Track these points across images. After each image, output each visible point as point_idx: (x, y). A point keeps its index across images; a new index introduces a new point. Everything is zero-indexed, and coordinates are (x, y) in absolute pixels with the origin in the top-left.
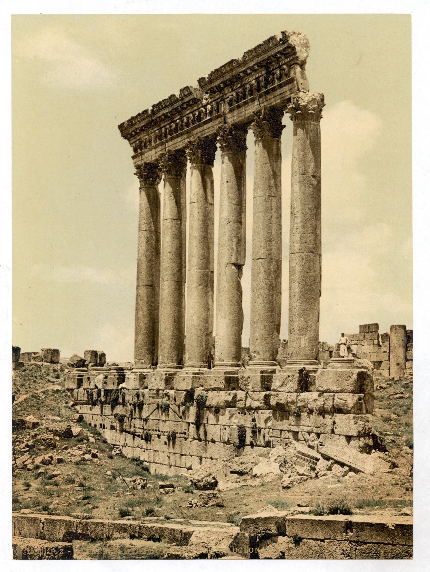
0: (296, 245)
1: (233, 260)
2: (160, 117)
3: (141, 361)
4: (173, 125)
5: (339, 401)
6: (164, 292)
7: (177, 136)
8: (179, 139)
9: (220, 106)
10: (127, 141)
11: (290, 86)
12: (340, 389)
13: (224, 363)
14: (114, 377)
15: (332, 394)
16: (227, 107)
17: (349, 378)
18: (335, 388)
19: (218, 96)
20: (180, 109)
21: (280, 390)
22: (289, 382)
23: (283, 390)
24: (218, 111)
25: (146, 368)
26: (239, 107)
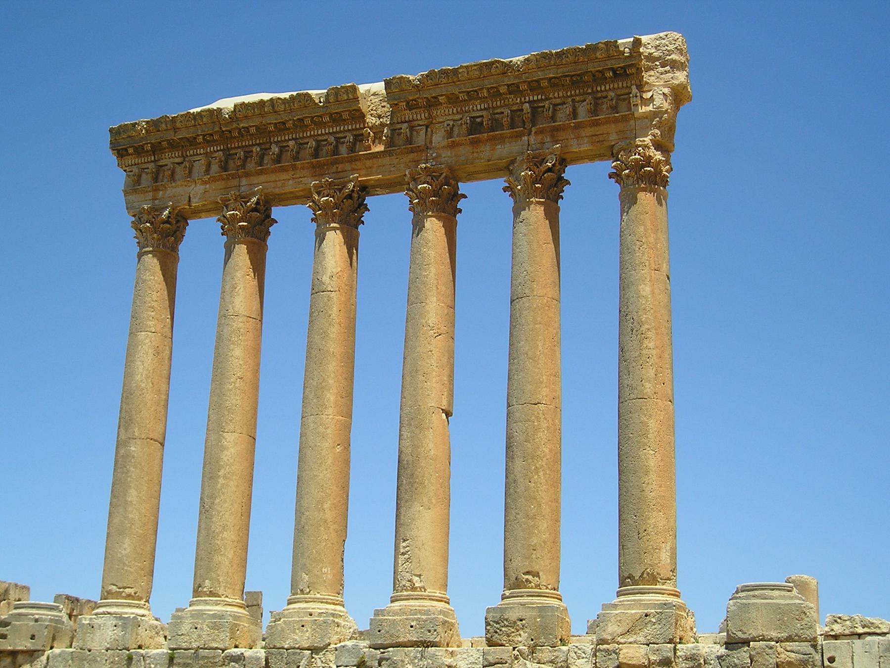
0: (647, 385)
1: (444, 405)
2: (247, 129)
3: (127, 590)
4: (275, 149)
5: (793, 655)
6: (225, 452)
7: (284, 170)
8: (284, 176)
9: (415, 133)
10: (114, 159)
11: (621, 126)
12: (785, 635)
13: (426, 593)
14: (33, 623)
15: (773, 643)
16: (438, 138)
17: (803, 616)
18: (774, 634)
19: (421, 116)
20: (307, 121)
21: (622, 641)
22: (649, 625)
23: (631, 640)
24: (409, 141)
25: (138, 607)
26: (474, 143)
